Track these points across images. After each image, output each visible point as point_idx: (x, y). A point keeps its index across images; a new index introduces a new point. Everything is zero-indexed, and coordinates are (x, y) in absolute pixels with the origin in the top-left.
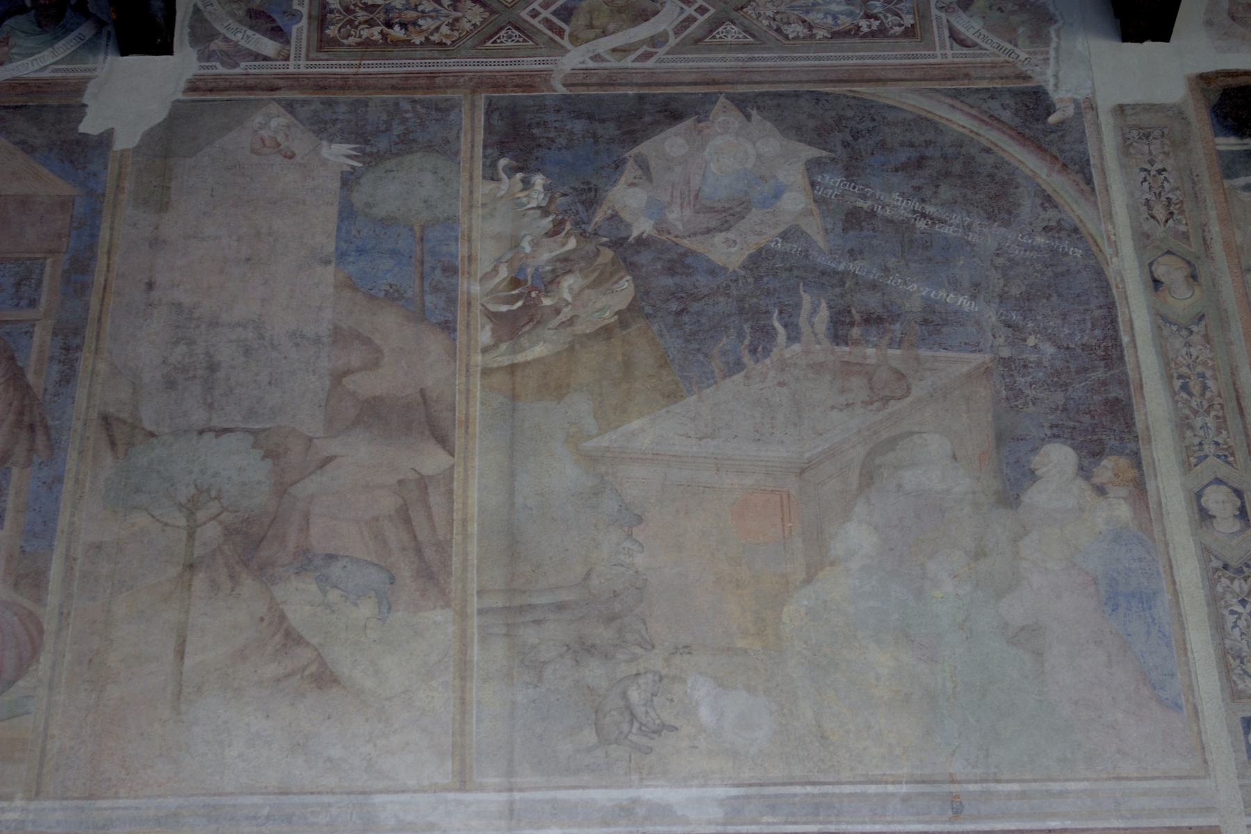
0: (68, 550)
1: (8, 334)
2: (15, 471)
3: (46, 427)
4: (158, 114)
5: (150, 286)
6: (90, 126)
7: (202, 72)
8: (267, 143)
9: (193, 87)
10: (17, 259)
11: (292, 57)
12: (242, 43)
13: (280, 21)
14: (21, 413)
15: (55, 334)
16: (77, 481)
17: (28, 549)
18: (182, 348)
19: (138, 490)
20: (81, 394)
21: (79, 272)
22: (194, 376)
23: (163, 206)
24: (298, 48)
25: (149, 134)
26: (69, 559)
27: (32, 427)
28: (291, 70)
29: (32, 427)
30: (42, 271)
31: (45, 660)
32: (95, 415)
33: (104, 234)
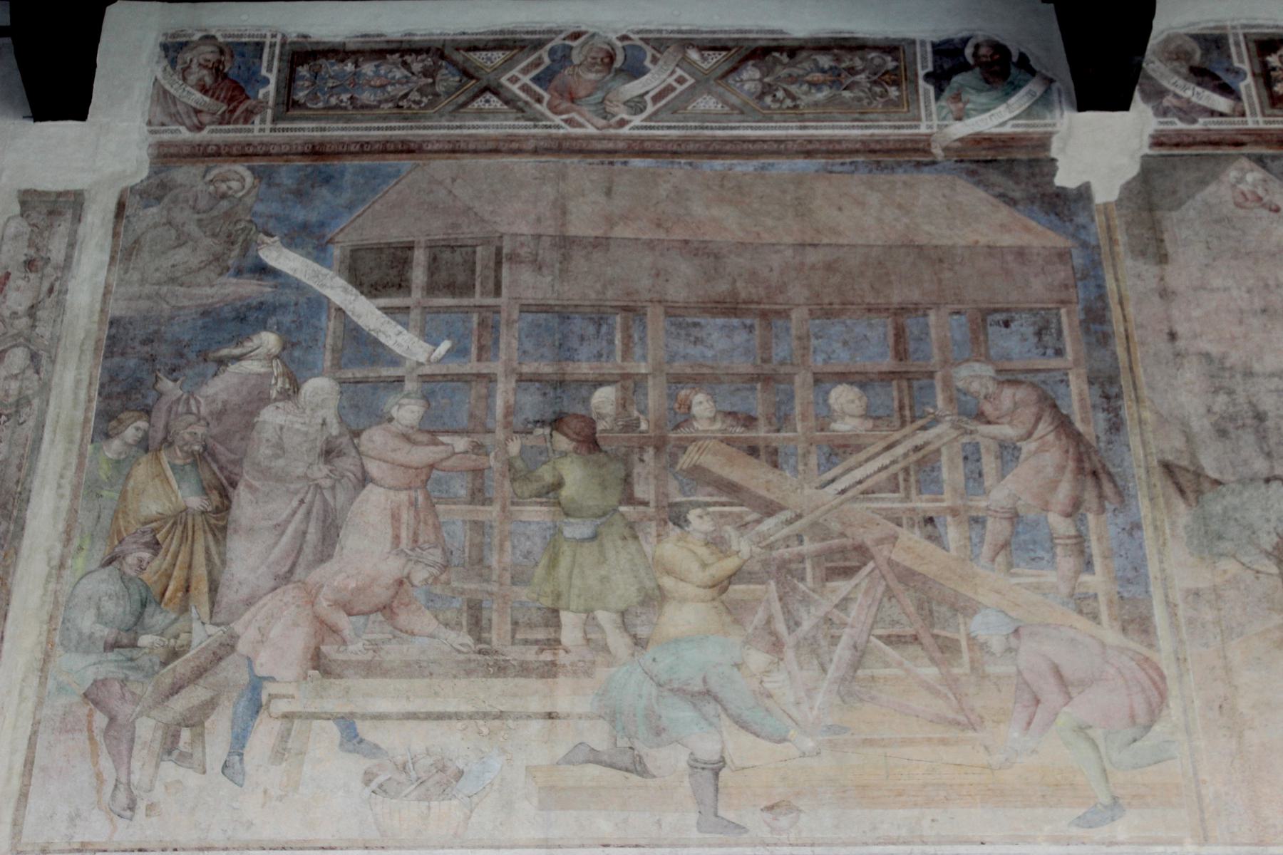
0: (1167, 596)
1: (1044, 382)
2: (1091, 517)
3: (1109, 474)
4: (1133, 170)
5: (1173, 336)
6: (1065, 179)
7: (1162, 127)
8: (1249, 196)
9: (1157, 142)
10: (1031, 310)
11: (1248, 112)
12: (1194, 99)
13: (1227, 78)
14: (1079, 460)
15: (1091, 382)
16: (1156, 528)
17: (1126, 595)
18: (1222, 398)
19: (1220, 537)
20: (1134, 441)
21: (1095, 319)
22: (1244, 425)
23: (1163, 259)
24: (1251, 105)
25: (1127, 187)
26: (1170, 606)
27: (1094, 474)
28: (1251, 125)
30: (1059, 322)
31: (1174, 705)
32: (1155, 463)
33: (1110, 284)
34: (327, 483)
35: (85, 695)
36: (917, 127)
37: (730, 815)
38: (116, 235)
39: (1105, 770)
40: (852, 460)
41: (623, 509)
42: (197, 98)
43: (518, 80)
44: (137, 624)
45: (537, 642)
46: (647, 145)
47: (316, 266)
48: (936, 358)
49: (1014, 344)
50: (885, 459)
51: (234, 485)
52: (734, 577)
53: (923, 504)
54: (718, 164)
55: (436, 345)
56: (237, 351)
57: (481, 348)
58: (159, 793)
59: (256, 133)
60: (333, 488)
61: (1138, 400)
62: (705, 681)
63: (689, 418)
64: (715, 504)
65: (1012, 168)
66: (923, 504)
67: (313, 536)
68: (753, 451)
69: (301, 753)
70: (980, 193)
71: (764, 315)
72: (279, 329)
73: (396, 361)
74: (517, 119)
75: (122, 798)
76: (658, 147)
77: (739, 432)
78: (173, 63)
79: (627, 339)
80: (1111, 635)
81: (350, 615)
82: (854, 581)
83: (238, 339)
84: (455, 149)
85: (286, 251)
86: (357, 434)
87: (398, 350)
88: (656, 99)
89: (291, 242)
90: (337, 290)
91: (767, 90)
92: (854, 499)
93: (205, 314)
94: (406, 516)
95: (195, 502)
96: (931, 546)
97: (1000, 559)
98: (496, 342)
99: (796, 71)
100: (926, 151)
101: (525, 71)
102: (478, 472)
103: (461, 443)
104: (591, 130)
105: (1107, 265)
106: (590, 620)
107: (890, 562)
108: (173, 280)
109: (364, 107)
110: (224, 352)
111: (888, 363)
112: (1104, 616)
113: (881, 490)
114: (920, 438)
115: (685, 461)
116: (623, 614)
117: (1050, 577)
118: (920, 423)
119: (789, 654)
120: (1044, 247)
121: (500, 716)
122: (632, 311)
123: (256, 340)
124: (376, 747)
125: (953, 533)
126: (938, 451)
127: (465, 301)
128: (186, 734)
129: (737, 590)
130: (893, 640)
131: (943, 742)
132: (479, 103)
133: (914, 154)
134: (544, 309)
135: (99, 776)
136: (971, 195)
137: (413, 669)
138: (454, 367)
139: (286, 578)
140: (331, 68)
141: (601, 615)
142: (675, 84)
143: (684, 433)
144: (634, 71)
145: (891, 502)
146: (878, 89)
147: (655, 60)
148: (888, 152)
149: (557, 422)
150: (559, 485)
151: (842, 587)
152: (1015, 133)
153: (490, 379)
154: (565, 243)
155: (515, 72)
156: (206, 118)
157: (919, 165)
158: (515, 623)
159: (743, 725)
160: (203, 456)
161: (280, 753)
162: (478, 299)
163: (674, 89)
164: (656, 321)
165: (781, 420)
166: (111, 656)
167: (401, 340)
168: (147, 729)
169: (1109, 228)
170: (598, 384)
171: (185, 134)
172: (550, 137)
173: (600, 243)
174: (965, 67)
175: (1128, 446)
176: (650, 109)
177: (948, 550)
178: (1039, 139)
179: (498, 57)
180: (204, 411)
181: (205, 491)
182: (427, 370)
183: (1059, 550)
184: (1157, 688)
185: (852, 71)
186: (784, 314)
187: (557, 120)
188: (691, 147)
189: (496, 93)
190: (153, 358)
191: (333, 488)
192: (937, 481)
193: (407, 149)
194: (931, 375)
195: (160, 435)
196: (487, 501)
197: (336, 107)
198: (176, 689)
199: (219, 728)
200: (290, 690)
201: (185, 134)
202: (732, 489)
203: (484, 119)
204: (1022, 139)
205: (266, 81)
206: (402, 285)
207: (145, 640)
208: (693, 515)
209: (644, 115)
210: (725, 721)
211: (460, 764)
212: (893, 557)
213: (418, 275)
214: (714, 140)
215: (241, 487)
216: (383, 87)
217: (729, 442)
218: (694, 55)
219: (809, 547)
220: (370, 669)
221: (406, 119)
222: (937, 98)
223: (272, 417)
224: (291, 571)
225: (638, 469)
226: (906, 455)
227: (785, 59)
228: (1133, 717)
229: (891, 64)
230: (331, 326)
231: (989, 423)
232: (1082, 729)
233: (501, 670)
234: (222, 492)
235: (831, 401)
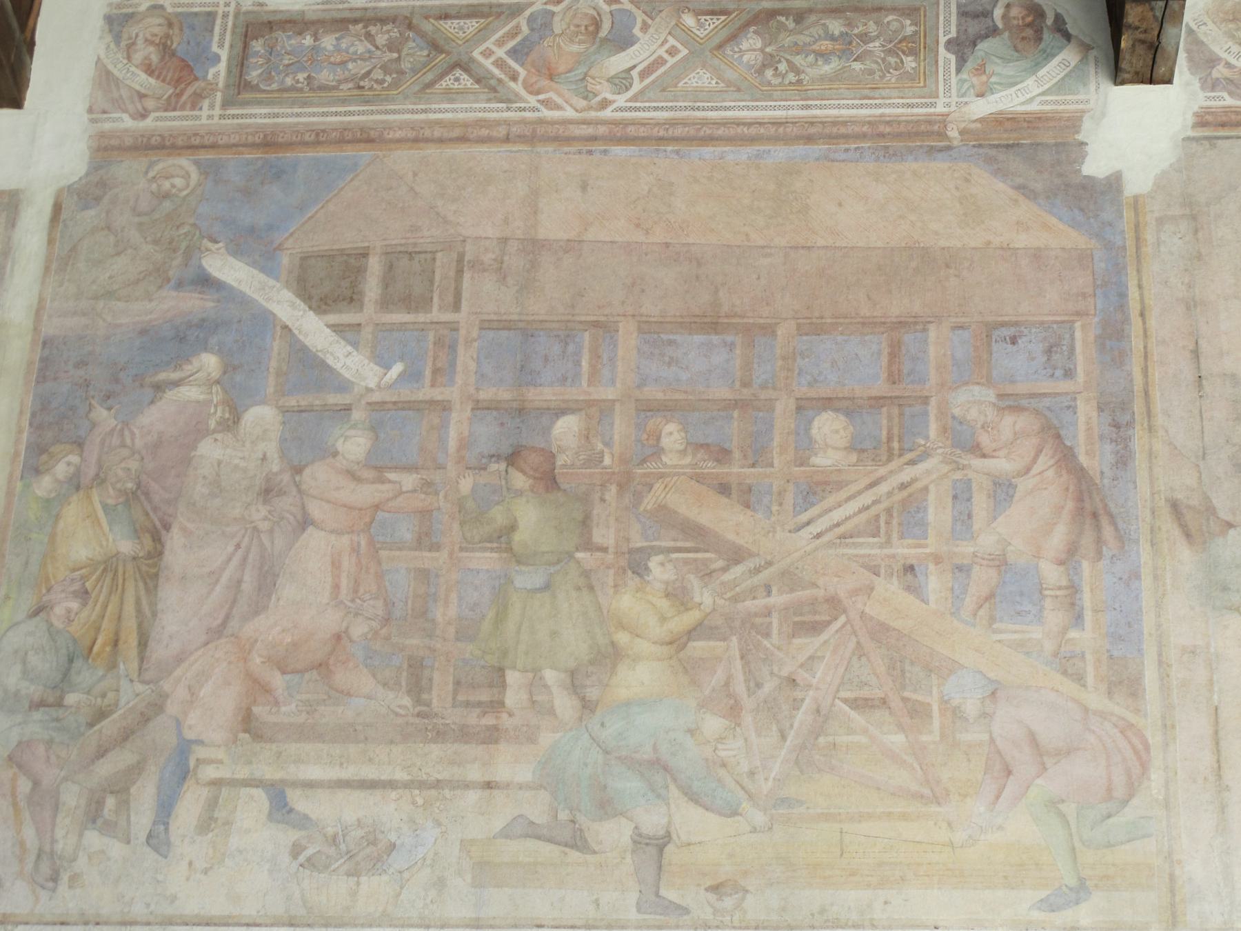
0: (1160, 655)
1: (1049, 409)
2: (1085, 565)
3: (1111, 516)
6: (1095, 166)
7: (1209, 103)
9: (1203, 120)
10: (1042, 323)
14: (1080, 499)
15: (1100, 409)
17: (1115, 653)
21: (1113, 338)
27: (1095, 515)
29: (1095, 515)
30: (1073, 338)
31: (1156, 776)
33: (1133, 293)
34: (264, 526)
35: (10, 758)
36: (933, 105)
37: (670, 894)
38: (51, 241)
39: (1073, 849)
40: (831, 500)
41: (579, 555)
42: (142, 80)
43: (491, 53)
44: (64, 681)
45: (479, 704)
46: (631, 131)
47: (262, 277)
48: (933, 378)
49: (1020, 364)
50: (867, 498)
51: (167, 527)
52: (692, 633)
53: (904, 550)
54: (708, 151)
55: (388, 368)
56: (175, 376)
57: (436, 371)
58: (81, 863)
59: (204, 121)
60: (271, 531)
61: (1150, 429)
62: (655, 748)
63: (658, 451)
64: (679, 550)
65: (1037, 154)
66: (904, 550)
67: (248, 586)
68: (724, 489)
69: (228, 823)
70: (1000, 186)
71: (747, 330)
72: (220, 352)
73: (343, 386)
74: (489, 101)
75: (45, 868)
76: (643, 132)
77: (710, 467)
78: (117, 38)
79: (596, 355)
80: (1095, 699)
81: (284, 673)
82: (824, 636)
83: (179, 361)
84: (418, 138)
85: (231, 260)
86: (298, 470)
87: (347, 374)
88: (643, 75)
89: (237, 250)
90: (285, 306)
91: (769, 62)
92: (831, 544)
93: (143, 332)
94: (347, 563)
95: (126, 546)
96: (910, 598)
97: (981, 613)
98: (453, 364)
99: (802, 39)
100: (942, 135)
101: (500, 43)
102: (425, 514)
103: (409, 481)
104: (569, 113)
105: (1131, 271)
106: (536, 683)
107: (863, 614)
108: (110, 295)
109: (323, 88)
110: (162, 376)
111: (880, 387)
112: (1090, 680)
113: (859, 535)
114: (905, 476)
115: (649, 502)
116: (573, 674)
117: (1036, 633)
118: (909, 456)
119: (748, 719)
120: (1063, 249)
121: (437, 785)
122: (604, 328)
123: (196, 363)
124: (306, 817)
125: (935, 583)
126: (926, 489)
127: (421, 317)
128: (110, 802)
129: (698, 647)
130: (861, 704)
131: (904, 817)
132: (447, 82)
133: (926, 138)
134: (507, 325)
135: (22, 844)
136: (988, 186)
137: (348, 733)
138: (406, 394)
139: (217, 632)
140: (287, 41)
141: (550, 675)
142: (666, 56)
143: (651, 467)
144: (622, 42)
145: (869, 548)
146: (892, 60)
147: (645, 27)
148: (898, 136)
149: (513, 458)
150: (512, 528)
151: (808, 645)
152: (1042, 112)
153: (444, 407)
154: (534, 247)
155: (489, 44)
156: (150, 104)
157: (931, 150)
158: (458, 683)
159: (693, 798)
160: (136, 495)
161: (207, 824)
162: (436, 314)
163: (664, 62)
164: (628, 339)
165: (758, 454)
166: (37, 715)
167: (352, 364)
168: (72, 797)
169: (1137, 226)
170: (562, 412)
171: (128, 122)
172: (523, 122)
173: (572, 246)
174: (993, 32)
175: (1135, 482)
176: (637, 86)
177: (927, 603)
178: (1069, 119)
179: (472, 25)
180: (139, 443)
181: (137, 533)
182: (377, 397)
183: (1048, 603)
184: (1139, 758)
185: (865, 38)
186: (769, 330)
187: (532, 101)
188: (679, 131)
189: (467, 70)
190: (87, 383)
191: (271, 531)
192: (923, 524)
193: (366, 138)
194: (925, 400)
195: (92, 472)
196: (435, 547)
197: (292, 89)
198: (101, 753)
199: (145, 795)
200: (220, 754)
201: (128, 122)
202: (697, 534)
203: (451, 101)
204: (1048, 119)
205: (217, 59)
206: (353, 299)
207: (71, 699)
208: (654, 563)
209: (630, 94)
210: (674, 791)
211: (393, 837)
212: (867, 610)
213: (372, 288)
214: (705, 123)
215: (175, 530)
216: (343, 63)
217: (699, 478)
218: (689, 20)
219: (778, 599)
220: (305, 733)
221: (367, 102)
222: (958, 71)
223: (210, 450)
224: (224, 624)
225: (597, 510)
226: (890, 494)
227: (791, 24)
228: (1109, 790)
229: (910, 30)
230: (276, 346)
231: (984, 456)
232: (1054, 804)
233: (440, 735)
234: (155, 535)
235: (814, 431)
